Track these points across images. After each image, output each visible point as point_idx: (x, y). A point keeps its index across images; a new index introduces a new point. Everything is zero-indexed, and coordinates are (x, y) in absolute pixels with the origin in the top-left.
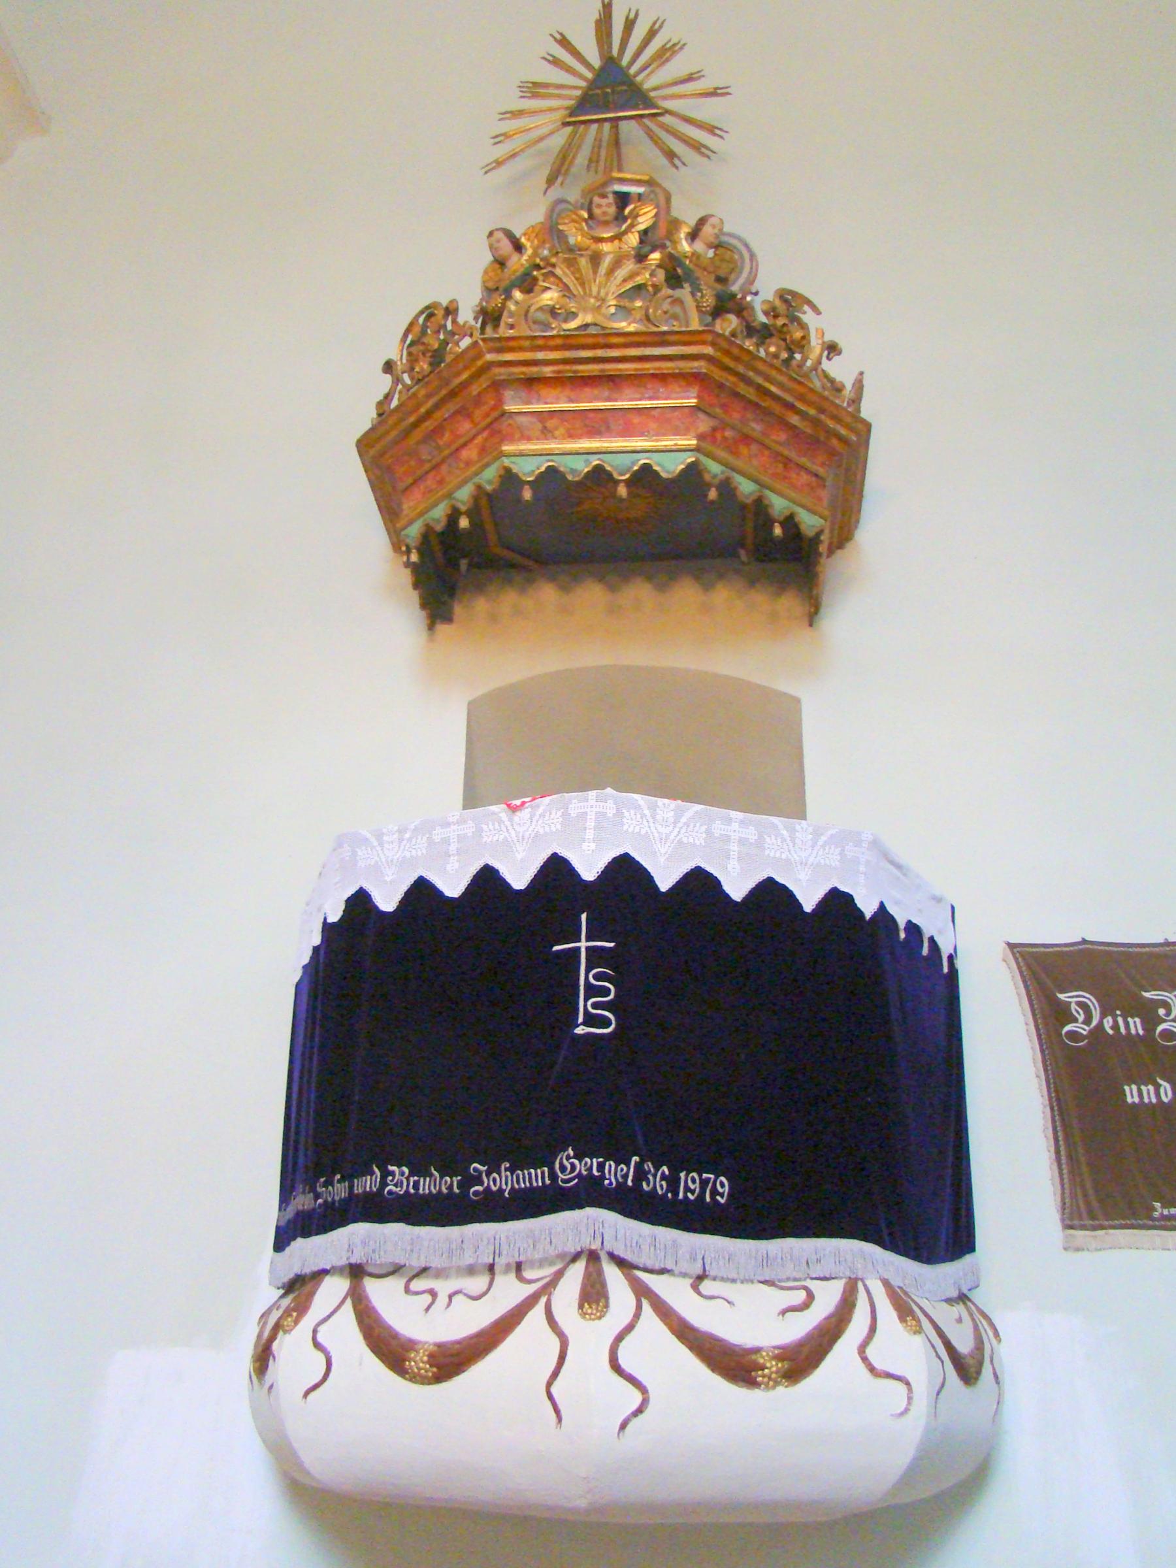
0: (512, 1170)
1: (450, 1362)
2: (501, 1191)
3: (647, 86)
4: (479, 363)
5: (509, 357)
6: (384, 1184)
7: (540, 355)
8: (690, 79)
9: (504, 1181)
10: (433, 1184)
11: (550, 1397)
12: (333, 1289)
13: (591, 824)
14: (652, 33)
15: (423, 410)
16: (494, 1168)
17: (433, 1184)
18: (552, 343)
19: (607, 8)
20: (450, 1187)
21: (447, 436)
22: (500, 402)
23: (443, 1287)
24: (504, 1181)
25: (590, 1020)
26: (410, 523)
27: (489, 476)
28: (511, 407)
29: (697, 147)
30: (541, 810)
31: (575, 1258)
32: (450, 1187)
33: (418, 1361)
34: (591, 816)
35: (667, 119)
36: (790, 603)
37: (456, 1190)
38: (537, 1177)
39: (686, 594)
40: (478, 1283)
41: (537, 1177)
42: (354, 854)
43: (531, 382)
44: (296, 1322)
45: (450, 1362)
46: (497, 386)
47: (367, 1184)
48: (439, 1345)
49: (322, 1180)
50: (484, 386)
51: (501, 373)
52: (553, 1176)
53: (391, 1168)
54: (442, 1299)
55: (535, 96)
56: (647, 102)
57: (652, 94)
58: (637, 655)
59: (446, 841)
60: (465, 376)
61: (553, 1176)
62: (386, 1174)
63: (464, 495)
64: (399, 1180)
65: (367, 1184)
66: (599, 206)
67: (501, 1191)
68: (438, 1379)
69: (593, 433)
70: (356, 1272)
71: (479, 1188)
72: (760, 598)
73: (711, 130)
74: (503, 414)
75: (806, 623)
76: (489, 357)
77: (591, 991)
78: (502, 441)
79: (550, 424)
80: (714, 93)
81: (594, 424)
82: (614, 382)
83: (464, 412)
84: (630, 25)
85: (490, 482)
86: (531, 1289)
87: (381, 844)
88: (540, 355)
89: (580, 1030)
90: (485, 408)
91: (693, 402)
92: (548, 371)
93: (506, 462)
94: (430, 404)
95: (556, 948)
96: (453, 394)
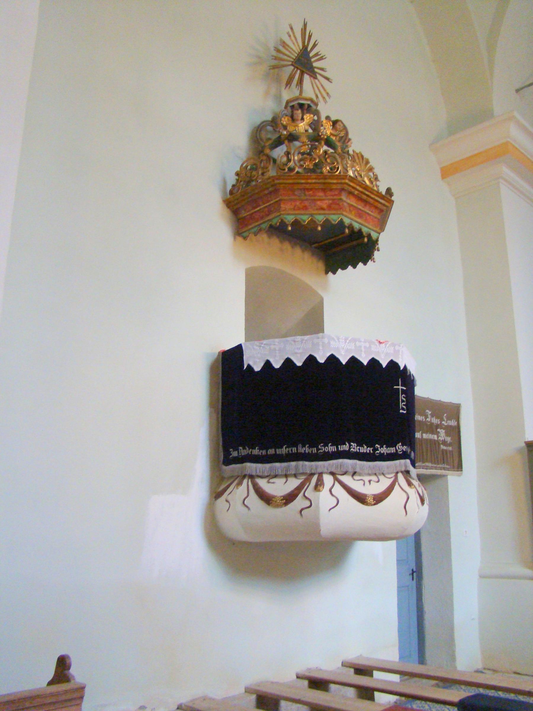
0: (387, 447)
1: (379, 499)
2: (384, 453)
3: (315, 65)
4: (343, 181)
5: (352, 184)
6: (350, 449)
7: (358, 187)
8: (322, 69)
9: (384, 450)
10: (365, 449)
11: (405, 507)
12: (328, 479)
13: (400, 353)
14: (315, 45)
15: (309, 181)
16: (382, 447)
17: (365, 449)
18: (362, 186)
19: (305, 25)
20: (370, 451)
21: (311, 192)
22: (340, 194)
23: (367, 479)
24: (384, 450)
25: (403, 409)
26: (288, 214)
27: (335, 218)
28: (344, 198)
29: (324, 98)
30: (388, 345)
31: (397, 473)
32: (370, 451)
33: (370, 500)
34: (401, 351)
35: (316, 81)
36: (321, 265)
37: (371, 452)
38: (392, 450)
39: (298, 251)
40: (374, 478)
41: (392, 450)
42: (329, 343)
43: (350, 193)
44: (323, 487)
45: (379, 499)
46: (343, 189)
47: (345, 447)
48: (374, 495)
49: (322, 444)
50: (338, 187)
51: (346, 187)
52: (396, 450)
53: (352, 444)
54: (367, 483)
55: (283, 47)
56: (315, 73)
57: (316, 70)
58: (288, 269)
59: (360, 347)
60: (335, 181)
61: (396, 450)
62: (350, 445)
63: (320, 218)
64: (355, 448)
65: (345, 447)
66: (340, 125)
67: (384, 453)
68: (375, 504)
69: (360, 217)
70: (332, 474)
71: (378, 452)
72: (315, 260)
73: (328, 94)
74: (341, 199)
75: (324, 272)
76: (347, 181)
77: (403, 401)
78: (341, 208)
79: (351, 209)
80: (327, 79)
81: (360, 214)
82: (366, 202)
83: (324, 190)
84: (310, 37)
85: (334, 220)
86: (392, 480)
87: (339, 341)
88: (358, 187)
89: (401, 411)
90: (333, 193)
91: (379, 217)
92: (356, 192)
93: (343, 217)
94: (314, 181)
95: (395, 387)
96: (324, 183)
